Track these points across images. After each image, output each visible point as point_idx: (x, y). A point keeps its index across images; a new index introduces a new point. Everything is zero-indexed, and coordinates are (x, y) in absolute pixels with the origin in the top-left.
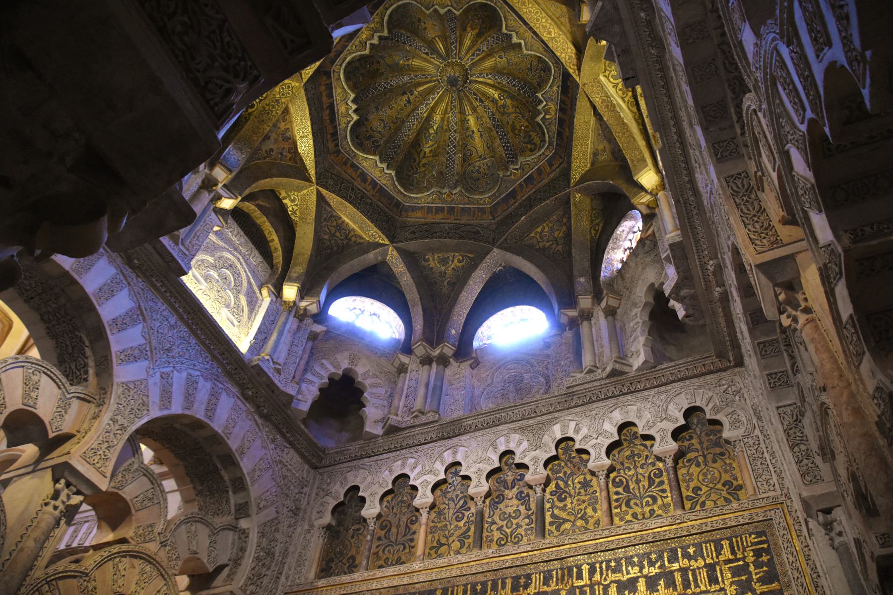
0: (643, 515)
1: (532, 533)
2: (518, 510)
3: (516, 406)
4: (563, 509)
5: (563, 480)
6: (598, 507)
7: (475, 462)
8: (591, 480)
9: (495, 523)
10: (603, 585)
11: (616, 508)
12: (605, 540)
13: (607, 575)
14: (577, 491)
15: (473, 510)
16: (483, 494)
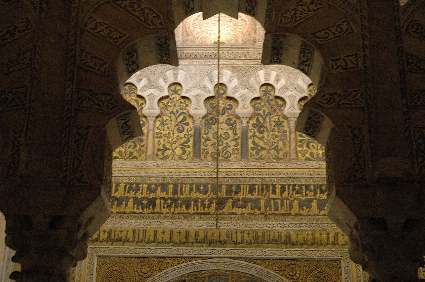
0: (318, 155)
1: (238, 153)
2: (227, 133)
3: (232, 48)
4: (262, 139)
5: (263, 117)
6: (287, 143)
7: (194, 88)
8: (283, 121)
9: (209, 140)
10: (289, 200)
11: (300, 146)
12: (293, 170)
13: (293, 194)
14: (272, 127)
15: (191, 125)
16: (201, 116)
